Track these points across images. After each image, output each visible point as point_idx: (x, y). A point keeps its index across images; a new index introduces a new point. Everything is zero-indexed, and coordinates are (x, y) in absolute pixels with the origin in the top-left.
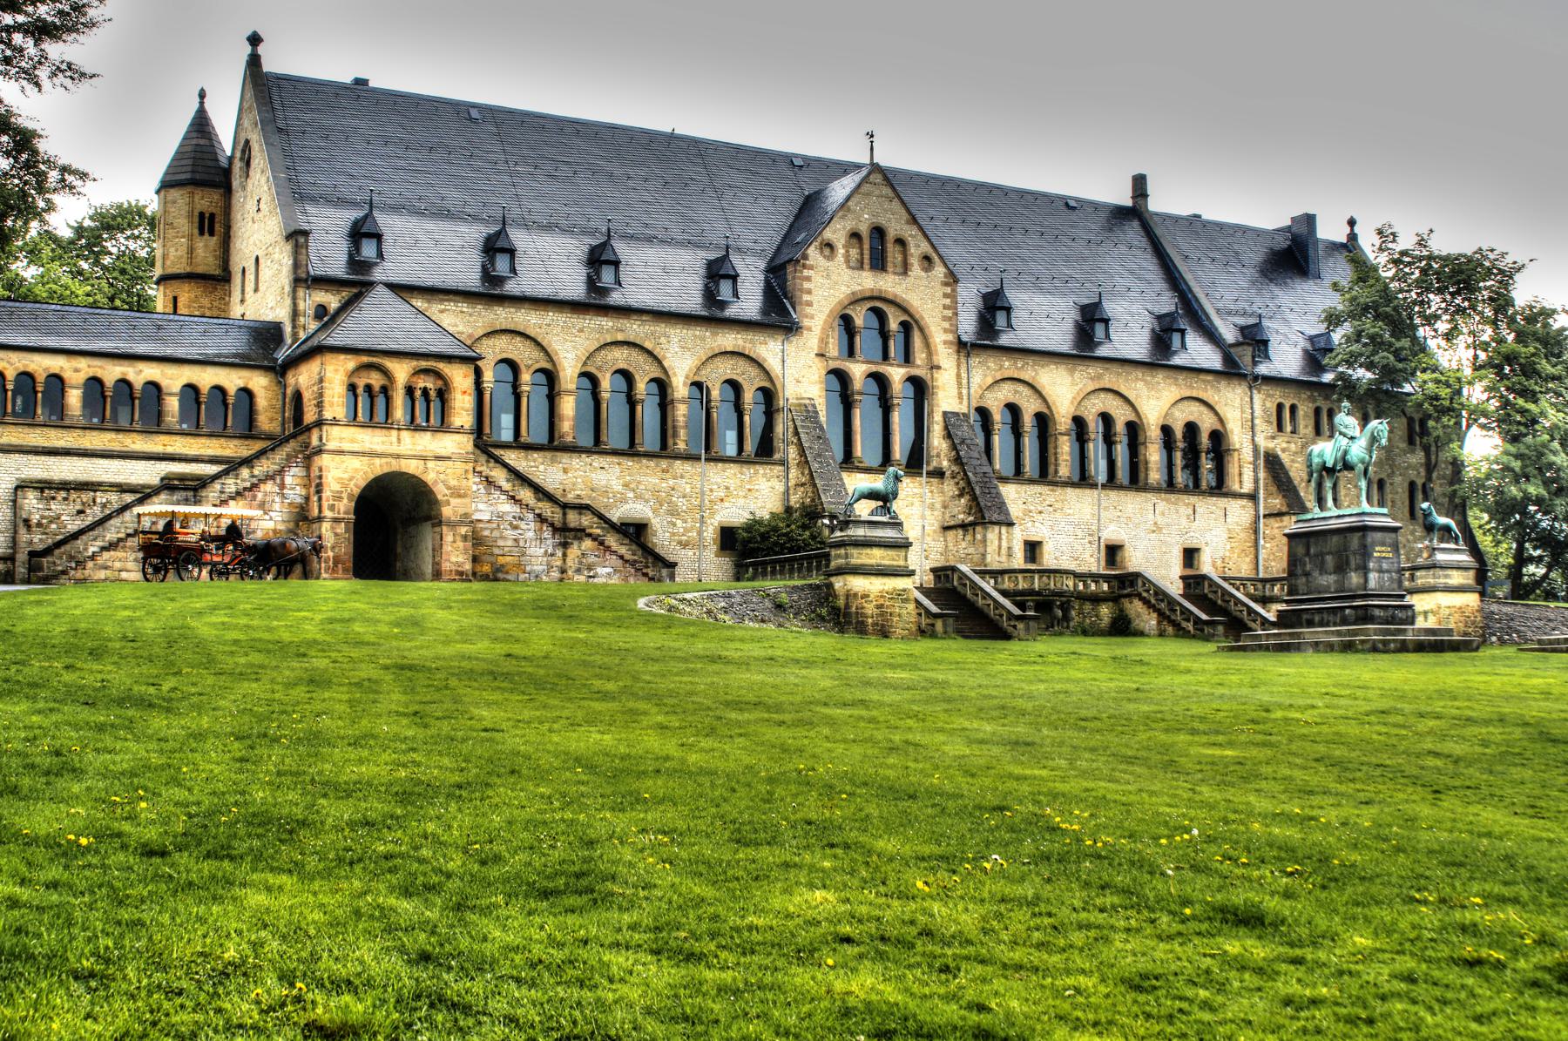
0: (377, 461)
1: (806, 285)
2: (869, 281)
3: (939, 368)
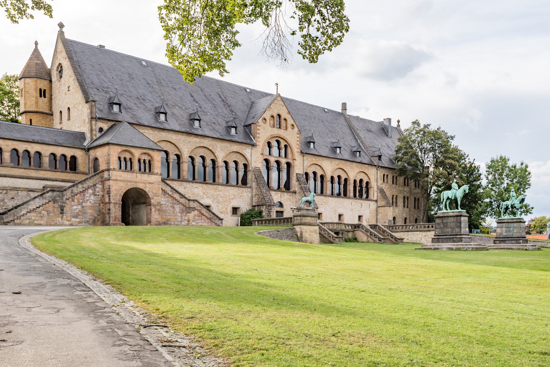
0: (129, 184)
1: (258, 131)
2: (276, 132)
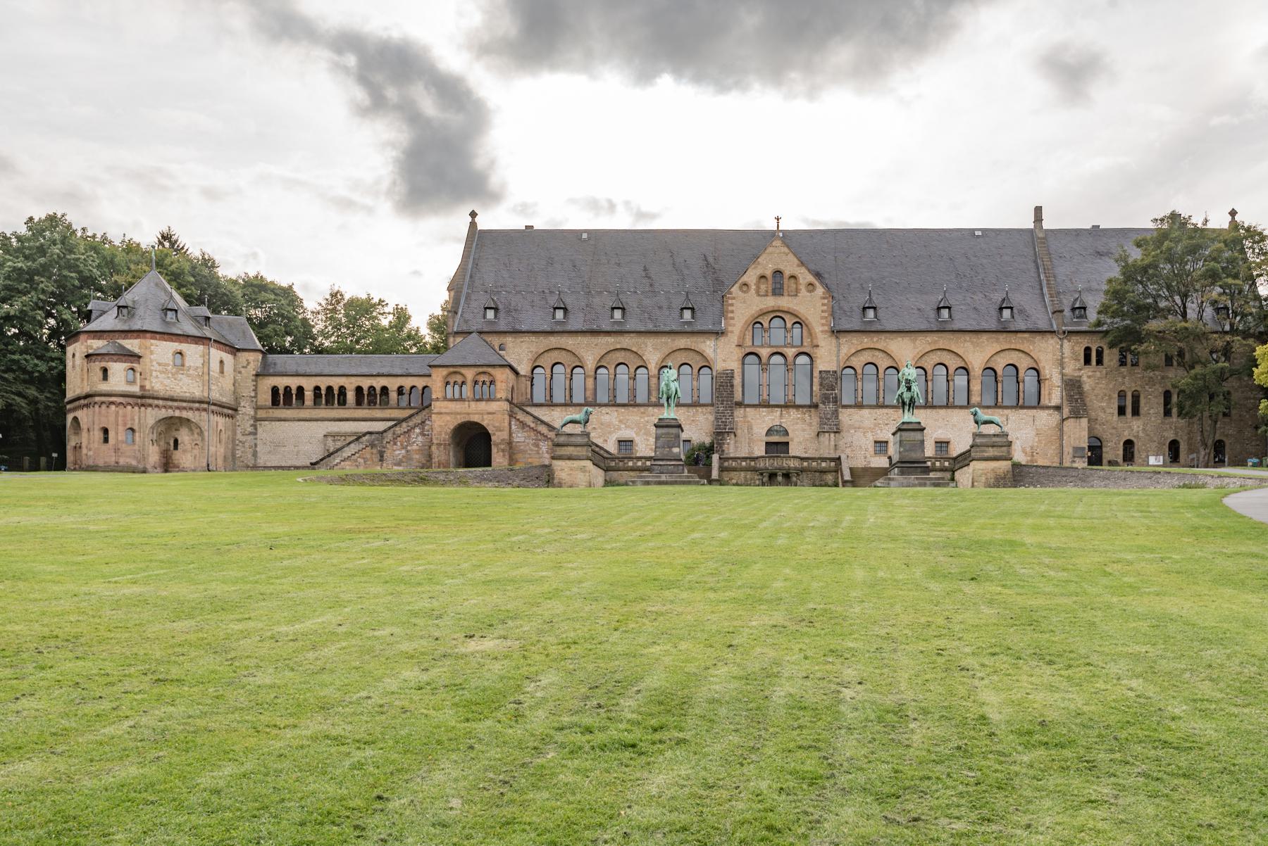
2: (771, 302)
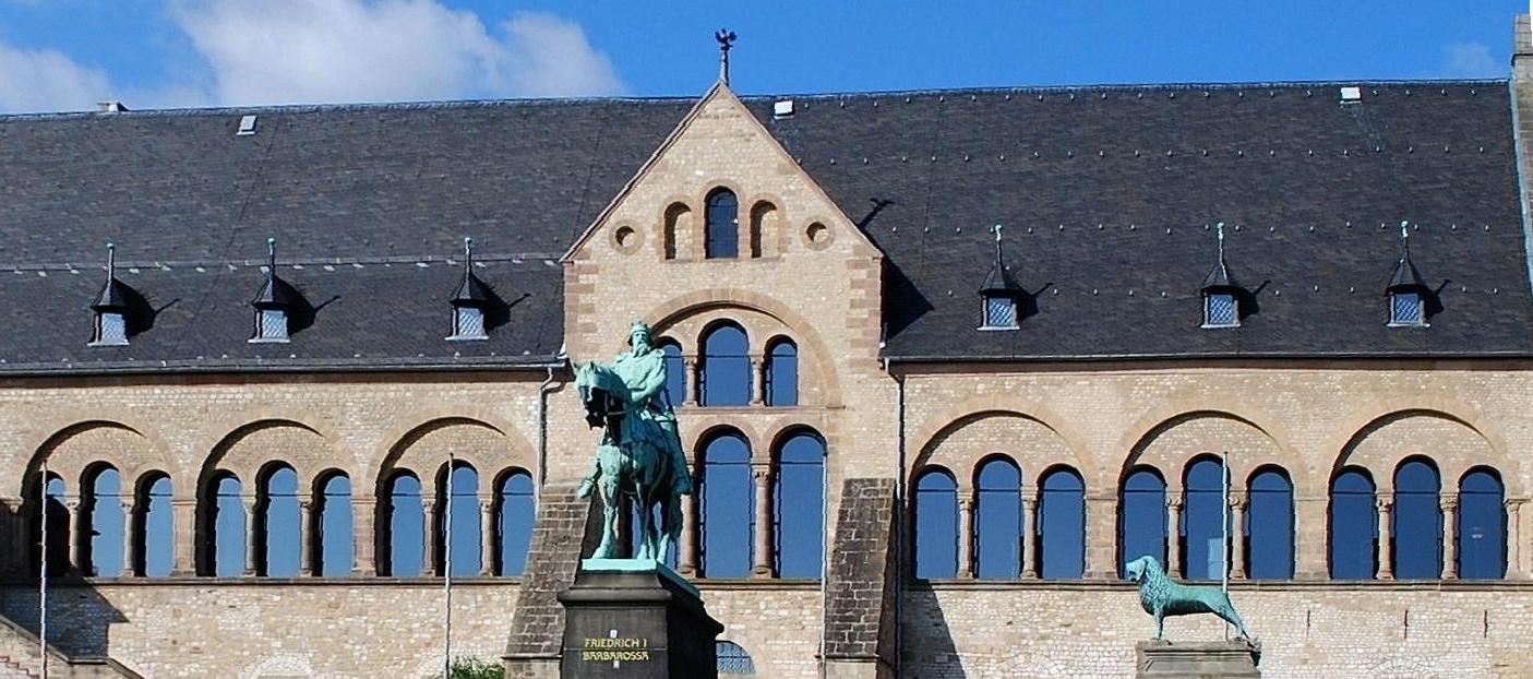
2: (701, 278)
3: (836, 407)
